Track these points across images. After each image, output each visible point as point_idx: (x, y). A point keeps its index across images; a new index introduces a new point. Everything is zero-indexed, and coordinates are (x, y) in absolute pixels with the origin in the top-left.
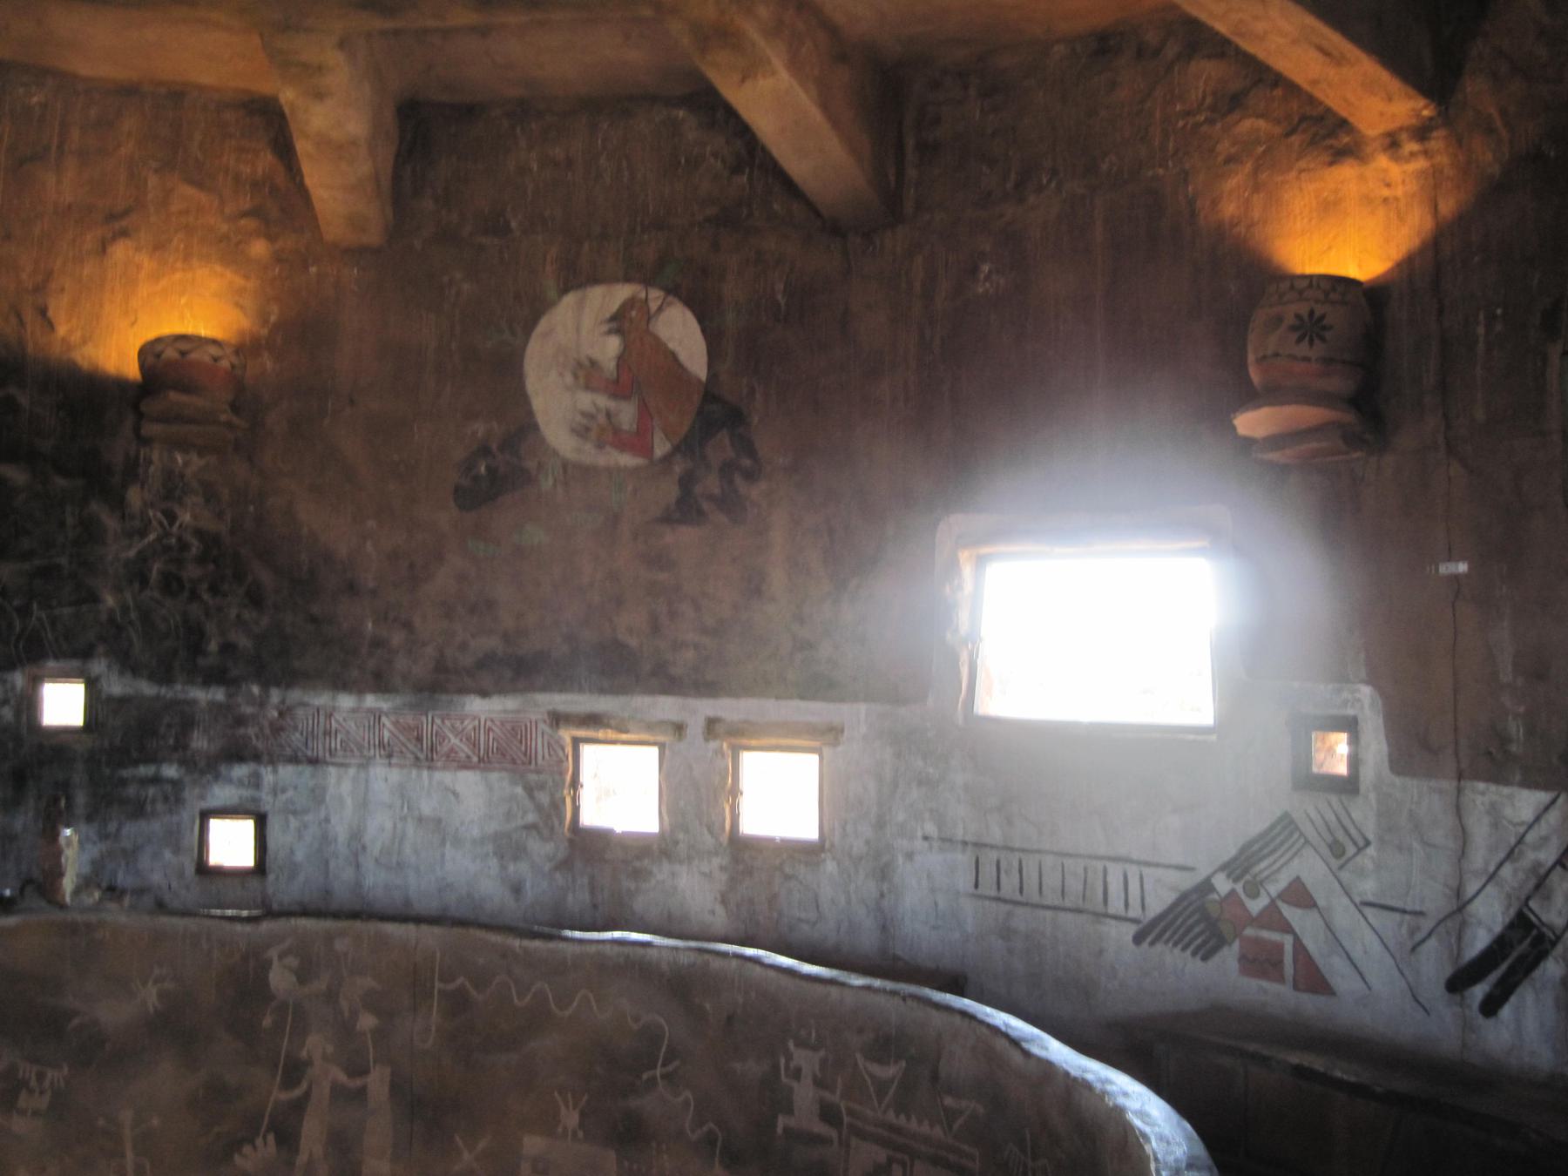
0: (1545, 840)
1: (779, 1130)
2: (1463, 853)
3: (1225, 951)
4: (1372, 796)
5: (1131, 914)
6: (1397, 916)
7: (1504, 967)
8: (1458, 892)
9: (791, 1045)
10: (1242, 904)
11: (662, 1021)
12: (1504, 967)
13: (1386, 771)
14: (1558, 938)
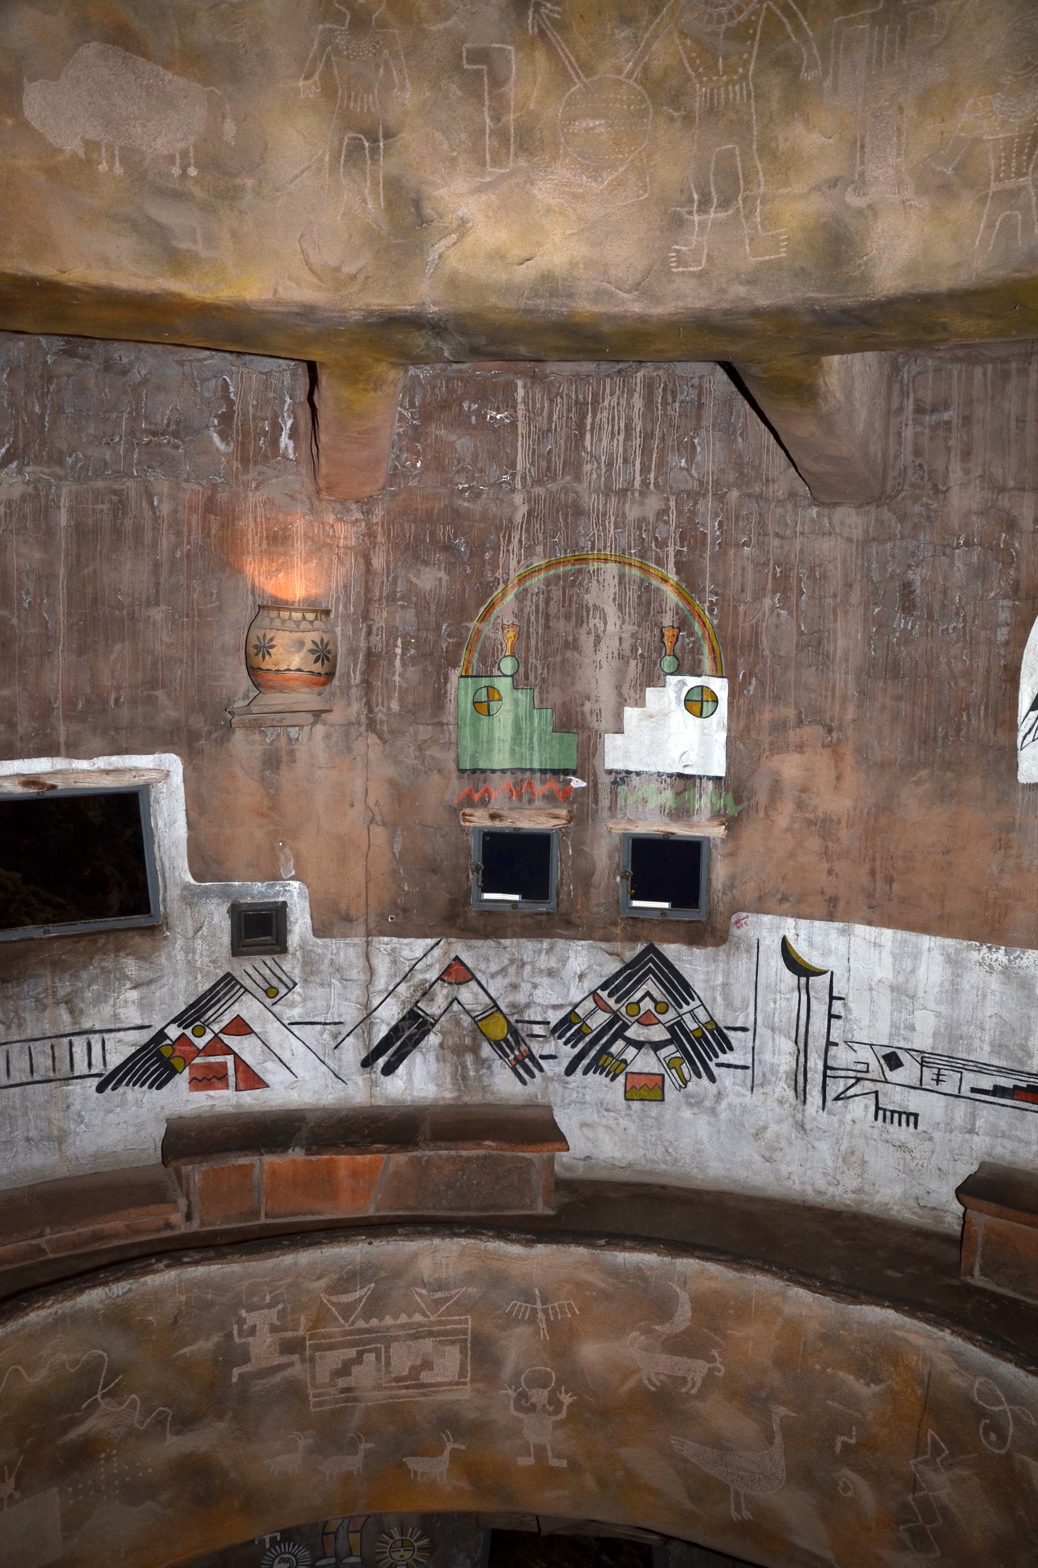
0: (430, 966)
1: (234, 1380)
2: (370, 982)
3: (177, 1077)
4: (299, 954)
5: (94, 1071)
6: (318, 1027)
7: (398, 1043)
8: (366, 1005)
9: (243, 1313)
10: (191, 1044)
11: (101, 1352)
12: (398, 1043)
13: (309, 934)
14: (436, 1021)
